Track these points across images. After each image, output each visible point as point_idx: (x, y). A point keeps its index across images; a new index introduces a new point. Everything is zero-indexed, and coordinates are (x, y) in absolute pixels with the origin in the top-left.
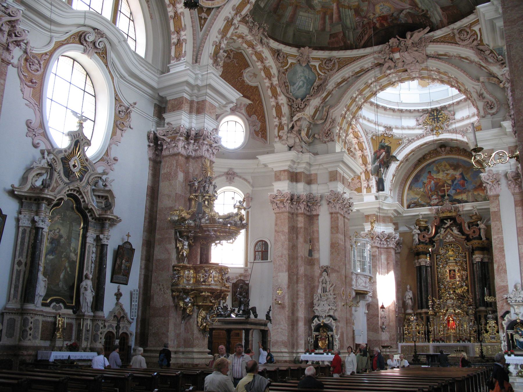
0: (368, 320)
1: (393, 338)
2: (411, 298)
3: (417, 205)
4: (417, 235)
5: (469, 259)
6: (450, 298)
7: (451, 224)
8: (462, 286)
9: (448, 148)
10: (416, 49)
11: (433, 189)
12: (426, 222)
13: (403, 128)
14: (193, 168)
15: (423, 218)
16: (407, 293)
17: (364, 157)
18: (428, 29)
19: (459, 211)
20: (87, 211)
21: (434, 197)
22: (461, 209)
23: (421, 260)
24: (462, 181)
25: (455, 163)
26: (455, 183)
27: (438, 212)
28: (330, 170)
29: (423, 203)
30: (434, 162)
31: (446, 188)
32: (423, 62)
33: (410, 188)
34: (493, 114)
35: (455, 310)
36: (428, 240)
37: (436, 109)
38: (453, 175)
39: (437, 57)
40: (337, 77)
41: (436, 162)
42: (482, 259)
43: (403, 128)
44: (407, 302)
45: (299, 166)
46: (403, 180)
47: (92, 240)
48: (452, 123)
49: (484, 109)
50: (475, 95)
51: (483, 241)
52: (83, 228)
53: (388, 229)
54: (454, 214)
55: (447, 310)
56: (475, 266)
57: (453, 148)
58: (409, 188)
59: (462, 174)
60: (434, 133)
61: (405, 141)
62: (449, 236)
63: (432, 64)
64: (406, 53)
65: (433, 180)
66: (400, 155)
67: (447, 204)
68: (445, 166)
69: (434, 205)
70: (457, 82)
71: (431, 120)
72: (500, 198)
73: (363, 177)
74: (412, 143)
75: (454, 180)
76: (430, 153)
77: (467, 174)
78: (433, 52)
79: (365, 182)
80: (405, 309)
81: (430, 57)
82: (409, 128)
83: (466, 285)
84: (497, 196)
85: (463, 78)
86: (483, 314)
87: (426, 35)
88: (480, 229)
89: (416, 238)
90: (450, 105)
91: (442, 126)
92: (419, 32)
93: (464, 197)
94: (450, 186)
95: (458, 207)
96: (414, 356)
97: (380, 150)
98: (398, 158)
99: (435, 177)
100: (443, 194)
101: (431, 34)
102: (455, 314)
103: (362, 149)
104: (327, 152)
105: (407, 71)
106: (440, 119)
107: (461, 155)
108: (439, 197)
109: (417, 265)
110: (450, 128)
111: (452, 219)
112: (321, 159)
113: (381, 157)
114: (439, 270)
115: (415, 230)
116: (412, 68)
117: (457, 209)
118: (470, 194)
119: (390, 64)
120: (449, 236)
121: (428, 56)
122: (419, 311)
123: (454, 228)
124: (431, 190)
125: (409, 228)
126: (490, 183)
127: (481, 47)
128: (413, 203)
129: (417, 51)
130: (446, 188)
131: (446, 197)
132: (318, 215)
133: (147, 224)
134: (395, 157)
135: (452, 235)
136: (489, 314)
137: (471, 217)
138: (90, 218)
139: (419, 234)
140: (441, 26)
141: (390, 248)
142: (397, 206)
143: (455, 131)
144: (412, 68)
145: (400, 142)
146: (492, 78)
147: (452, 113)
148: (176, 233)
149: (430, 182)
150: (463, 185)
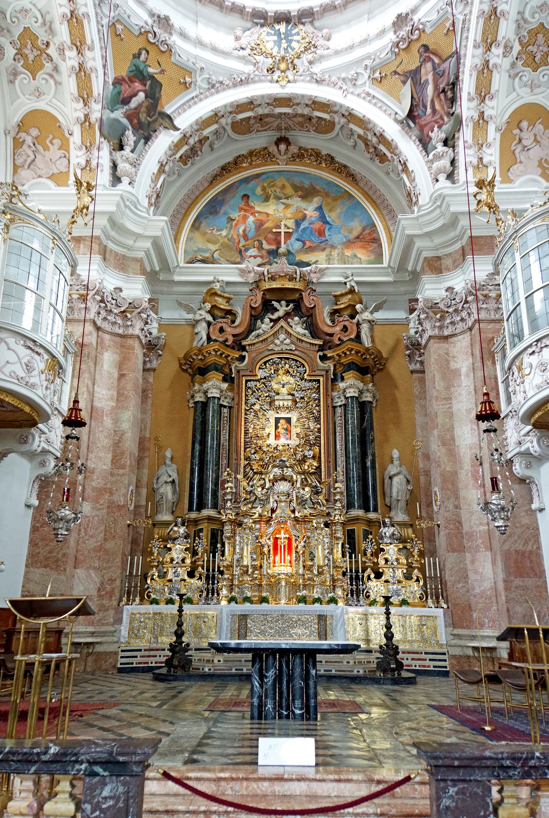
0: (34, 529)
1: (108, 588)
2: (173, 482)
4: (204, 325)
5: (327, 395)
6: (284, 478)
7: (288, 315)
8: (304, 459)
9: (294, 149)
12: (228, 300)
13: (200, 43)
16: (163, 469)
17: (82, 73)
21: (253, 252)
22: (314, 278)
23: (210, 384)
24: (318, 225)
25: (307, 183)
26: (302, 227)
30: (258, 176)
31: (283, 230)
33: (196, 226)
35: (293, 512)
36: (231, 340)
41: (263, 176)
42: (361, 392)
43: (200, 43)
44: (162, 490)
48: (322, 58)
51: (368, 349)
55: (273, 511)
56: (339, 411)
57: (306, 150)
58: (193, 225)
59: (319, 209)
60: (275, 77)
61: (200, 80)
62: (282, 336)
66: (184, 116)
68: (283, 187)
73: (76, 139)
74: (218, 92)
76: (251, 153)
77: (330, 211)
79: (80, 153)
80: (156, 510)
82: (215, 50)
83: (314, 457)
86: (359, 529)
88: (358, 324)
89: (202, 329)
91: (296, 61)
96: (172, 648)
97: (131, 80)
98: (176, 123)
99: (257, 209)
100: (274, 247)
102: (296, 519)
103: (79, 44)
106: (294, 44)
108: (264, 252)
109: (200, 398)
113: (134, 103)
114: (251, 417)
115: (202, 312)
118: (335, 253)
120: (282, 336)
122: (193, 515)
123: (296, 318)
131: (282, 250)
134: (170, 118)
135: (289, 335)
136: (385, 525)
139: (209, 324)
141: (132, 336)
142: (163, 230)
145: (188, 79)
149: (245, 218)
150: (321, 233)
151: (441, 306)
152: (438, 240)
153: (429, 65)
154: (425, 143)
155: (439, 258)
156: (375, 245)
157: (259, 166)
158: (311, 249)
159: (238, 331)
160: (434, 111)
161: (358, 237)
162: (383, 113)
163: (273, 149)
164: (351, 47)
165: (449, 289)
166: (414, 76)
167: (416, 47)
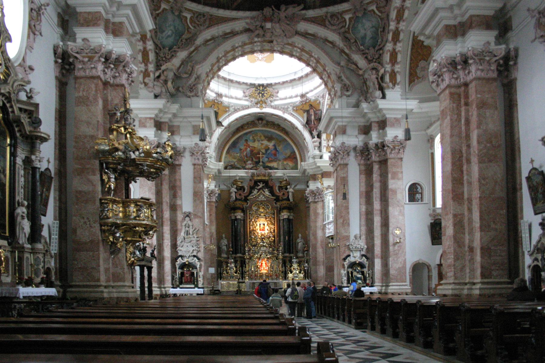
3: (233, 167)
7: (263, 186)
9: (264, 122)
10: (288, 23)
11: (249, 155)
12: (242, 182)
14: (115, 97)
15: (239, 179)
18: (302, 6)
19: (271, 176)
20: (15, 125)
21: (249, 162)
24: (274, 152)
25: (269, 135)
27: (253, 175)
28: (194, 124)
29: (238, 166)
31: (261, 156)
32: (290, 37)
33: (228, 152)
34: (349, 96)
37: (263, 85)
38: (267, 146)
39: (305, 35)
40: (207, 34)
45: (165, 116)
46: (221, 144)
47: (21, 161)
48: (275, 100)
49: (341, 90)
50: (333, 77)
52: (10, 145)
53: (212, 186)
54: (267, 178)
57: (269, 122)
59: (274, 146)
60: (258, 106)
63: (299, 41)
64: (278, 25)
65: (249, 147)
67: (261, 170)
68: (261, 137)
69: (248, 169)
70: (318, 61)
71: (257, 94)
72: (349, 166)
75: (267, 149)
77: (279, 146)
78: (302, 30)
81: (299, 34)
84: (347, 165)
85: (325, 59)
87: (299, 12)
90: (276, 84)
91: (266, 101)
92: (294, 7)
93: (274, 164)
94: (263, 154)
95: (271, 173)
99: (251, 145)
101: (303, 12)
104: (191, 106)
105: (272, 42)
107: (276, 130)
110: (272, 104)
111: (266, 183)
112: (188, 112)
115: (233, 189)
116: (279, 40)
117: (270, 175)
118: (280, 163)
119: (260, 32)
121: (297, 33)
124: (246, 156)
125: (227, 186)
126: (342, 153)
127: (347, 35)
128: (231, 166)
129: (288, 24)
130: (261, 156)
131: (261, 163)
132: (180, 165)
133: (57, 151)
137: (281, 182)
138: (18, 134)
140: (314, 7)
143: (275, 108)
144: (279, 40)
146: (350, 64)
147: (276, 91)
148: (101, 164)
149: (246, 149)
150: (275, 155)
151: (315, 192)
152: (314, 170)
153: (312, 110)
154: (311, 134)
155: (315, 175)
156: (294, 160)
157: (250, 128)
158: (270, 161)
159: (245, 195)
160: (314, 124)
161: (289, 157)
162: (297, 122)
163: (256, 122)
164: (286, 98)
165: (318, 188)
166: (308, 112)
167: (308, 104)
